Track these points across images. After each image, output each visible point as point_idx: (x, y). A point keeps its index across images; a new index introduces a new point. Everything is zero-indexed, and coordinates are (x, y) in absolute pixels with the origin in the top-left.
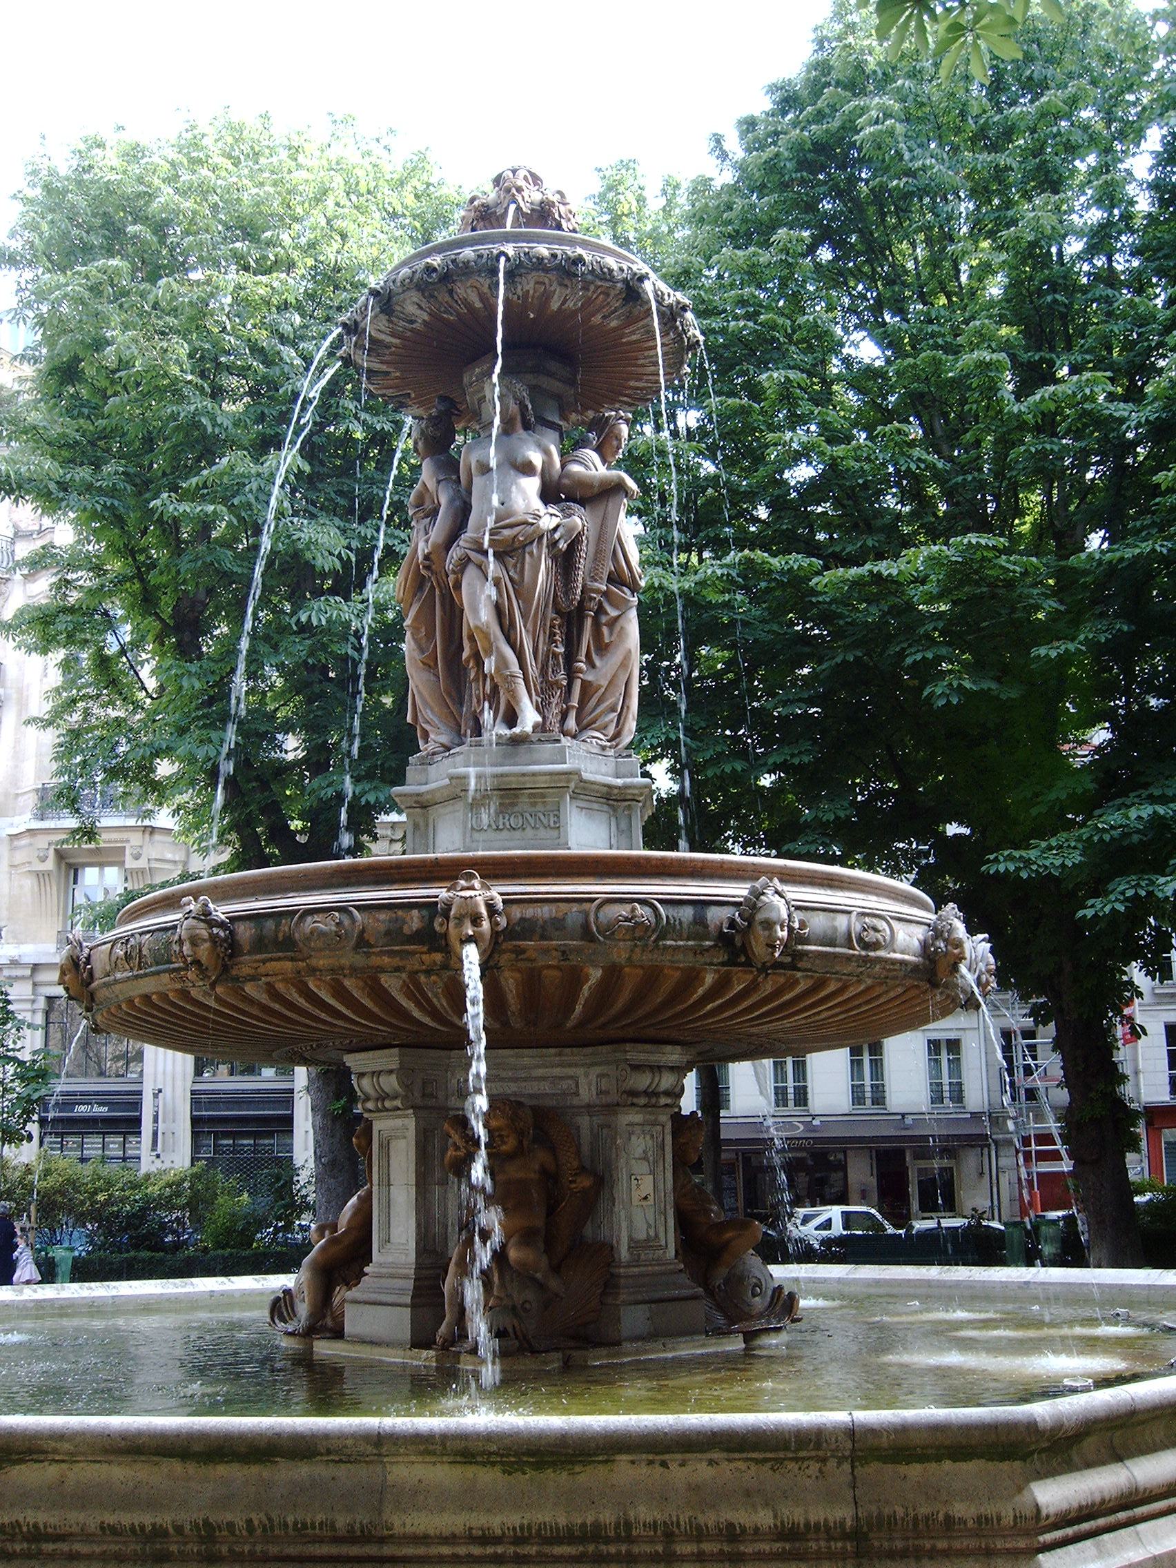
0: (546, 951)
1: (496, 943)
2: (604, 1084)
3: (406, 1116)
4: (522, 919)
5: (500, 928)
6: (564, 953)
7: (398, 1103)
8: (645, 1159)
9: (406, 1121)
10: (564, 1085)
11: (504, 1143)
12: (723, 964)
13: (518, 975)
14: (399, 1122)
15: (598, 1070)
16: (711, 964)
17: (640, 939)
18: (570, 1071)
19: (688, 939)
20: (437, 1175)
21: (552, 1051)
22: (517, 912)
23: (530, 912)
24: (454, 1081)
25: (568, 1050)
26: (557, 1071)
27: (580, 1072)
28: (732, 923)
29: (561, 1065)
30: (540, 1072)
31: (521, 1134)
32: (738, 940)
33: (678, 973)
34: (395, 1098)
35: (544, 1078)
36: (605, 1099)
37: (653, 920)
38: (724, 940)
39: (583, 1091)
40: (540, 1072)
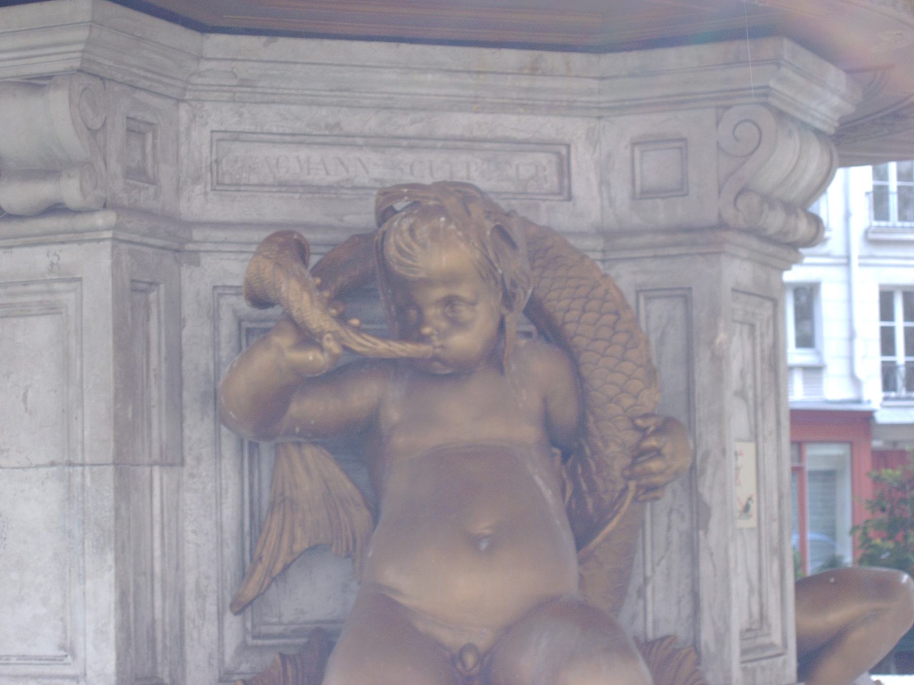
2: (656, 168)
3: (77, 237)
7: (69, 190)
8: (741, 394)
9: (69, 255)
10: (524, 166)
11: (457, 324)
14: (37, 259)
15: (638, 124)
18: (547, 126)
20: (159, 427)
21: (511, 57)
24: (200, 137)
25: (554, 59)
26: (513, 124)
27: (573, 129)
29: (530, 108)
30: (461, 123)
31: (508, 299)
34: (49, 170)
35: (468, 143)
36: (661, 213)
39: (584, 184)
40: (461, 123)
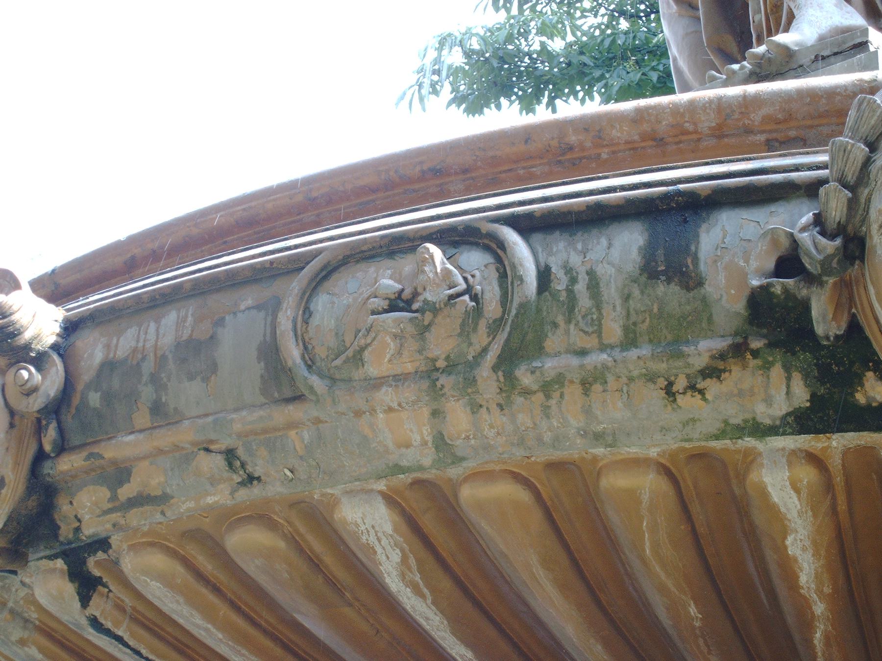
0: (183, 458)
1: (40, 457)
4: (109, 366)
5: (37, 403)
6: (230, 455)
12: (802, 422)
13: (158, 560)
16: (761, 431)
17: (451, 368)
19: (630, 340)
22: (93, 350)
23: (127, 341)
28: (789, 263)
32: (825, 320)
33: (649, 484)
37: (491, 293)
38: (774, 322)
